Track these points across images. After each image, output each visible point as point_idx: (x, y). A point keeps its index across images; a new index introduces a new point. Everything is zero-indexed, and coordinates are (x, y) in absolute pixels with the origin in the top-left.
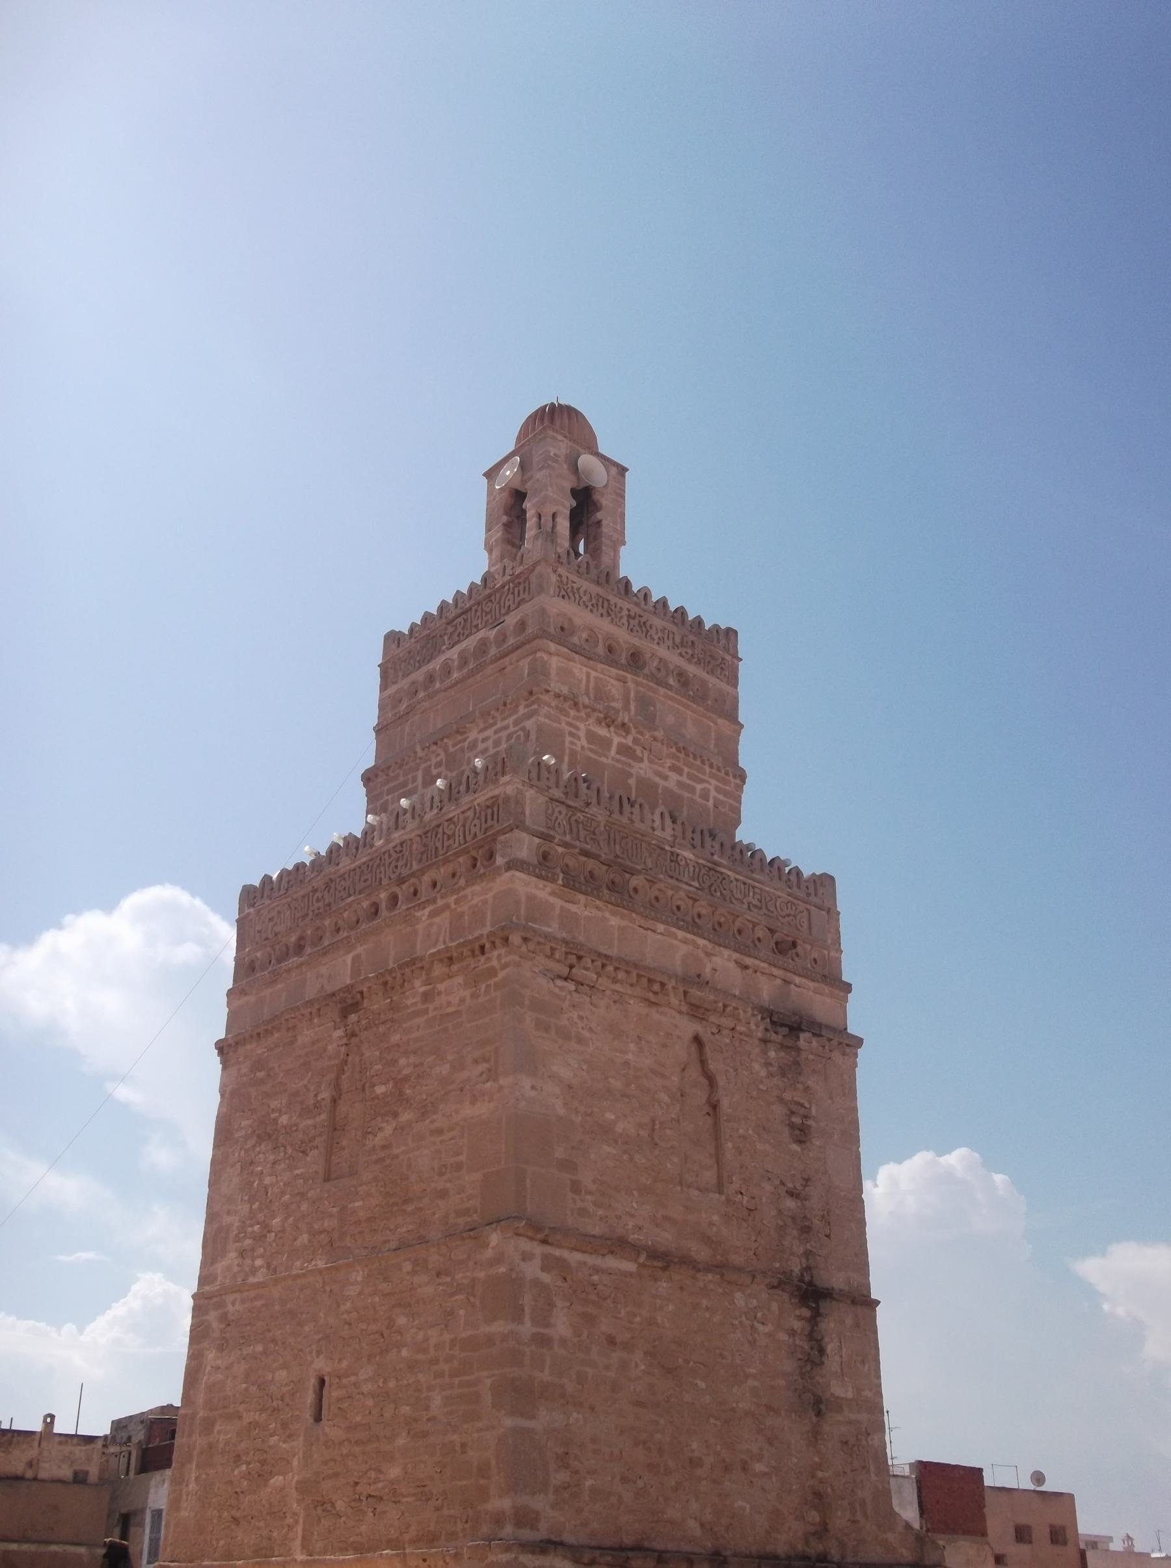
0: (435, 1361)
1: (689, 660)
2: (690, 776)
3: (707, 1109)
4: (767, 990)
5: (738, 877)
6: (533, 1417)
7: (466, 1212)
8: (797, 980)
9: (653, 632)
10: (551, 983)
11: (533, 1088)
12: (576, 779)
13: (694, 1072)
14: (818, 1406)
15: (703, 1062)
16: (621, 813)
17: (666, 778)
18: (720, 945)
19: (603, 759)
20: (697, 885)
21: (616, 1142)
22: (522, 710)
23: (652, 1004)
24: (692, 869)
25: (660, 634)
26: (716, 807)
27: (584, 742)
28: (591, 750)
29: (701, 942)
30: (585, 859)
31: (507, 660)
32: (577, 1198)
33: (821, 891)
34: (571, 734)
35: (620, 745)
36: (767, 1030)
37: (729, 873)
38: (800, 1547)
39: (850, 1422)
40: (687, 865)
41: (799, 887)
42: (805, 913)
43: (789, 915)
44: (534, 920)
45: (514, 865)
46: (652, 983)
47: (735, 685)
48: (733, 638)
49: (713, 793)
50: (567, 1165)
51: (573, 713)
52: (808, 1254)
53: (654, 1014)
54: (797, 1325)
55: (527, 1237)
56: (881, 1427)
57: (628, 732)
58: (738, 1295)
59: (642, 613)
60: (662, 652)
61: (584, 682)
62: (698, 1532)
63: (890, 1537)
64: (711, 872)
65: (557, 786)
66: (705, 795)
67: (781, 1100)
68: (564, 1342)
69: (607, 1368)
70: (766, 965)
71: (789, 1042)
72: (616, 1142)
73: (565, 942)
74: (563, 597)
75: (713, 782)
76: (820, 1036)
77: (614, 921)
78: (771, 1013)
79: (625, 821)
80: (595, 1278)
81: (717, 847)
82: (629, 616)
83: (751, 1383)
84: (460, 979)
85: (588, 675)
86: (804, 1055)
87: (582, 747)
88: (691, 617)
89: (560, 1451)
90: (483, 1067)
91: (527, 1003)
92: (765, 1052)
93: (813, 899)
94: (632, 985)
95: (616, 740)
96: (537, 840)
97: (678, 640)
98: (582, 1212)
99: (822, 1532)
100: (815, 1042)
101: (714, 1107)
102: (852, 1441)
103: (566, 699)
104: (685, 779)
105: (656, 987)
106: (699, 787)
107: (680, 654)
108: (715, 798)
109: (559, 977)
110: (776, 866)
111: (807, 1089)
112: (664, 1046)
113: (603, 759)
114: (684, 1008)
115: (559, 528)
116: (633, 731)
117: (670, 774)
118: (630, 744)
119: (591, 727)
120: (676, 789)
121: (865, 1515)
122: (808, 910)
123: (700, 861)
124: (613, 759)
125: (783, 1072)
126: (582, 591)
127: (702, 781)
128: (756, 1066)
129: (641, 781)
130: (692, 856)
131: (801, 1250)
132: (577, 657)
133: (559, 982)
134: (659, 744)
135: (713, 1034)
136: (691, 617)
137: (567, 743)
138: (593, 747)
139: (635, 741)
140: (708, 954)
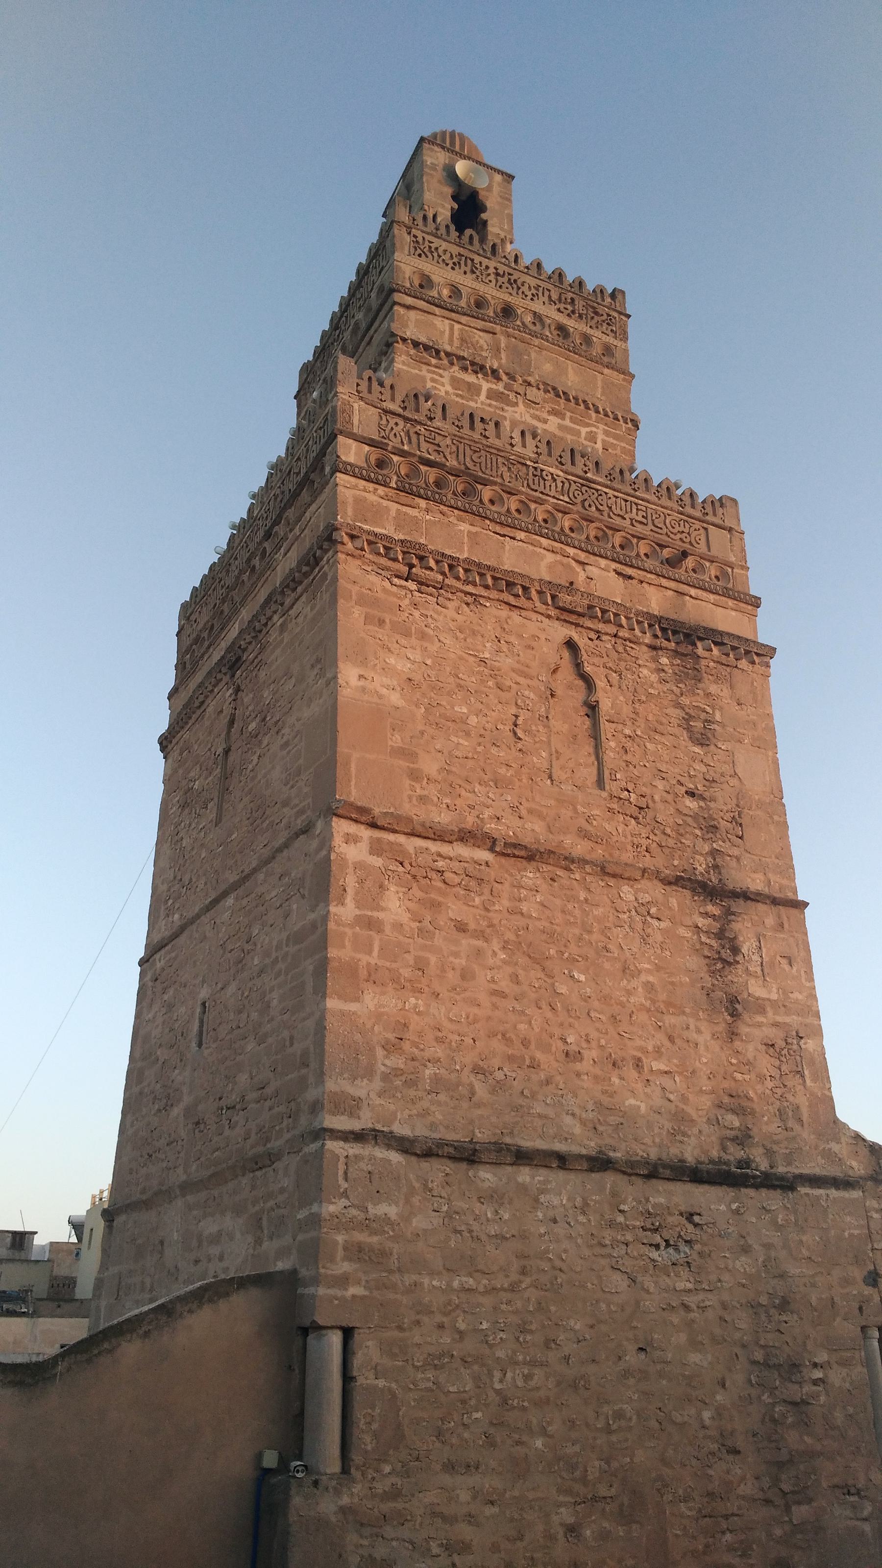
1: (568, 315)
2: (572, 420)
3: (584, 710)
4: (656, 600)
5: (616, 494)
6: (357, 999)
8: (693, 592)
9: (525, 288)
10: (387, 584)
11: (361, 677)
12: (416, 396)
13: (567, 673)
14: (734, 1007)
17: (545, 421)
18: (595, 554)
20: (567, 500)
24: (560, 485)
25: (534, 291)
27: (449, 388)
28: (457, 395)
29: (571, 551)
30: (427, 468)
32: (418, 786)
33: (720, 511)
34: (433, 380)
35: (489, 390)
37: (607, 490)
38: (715, 1154)
39: (776, 1025)
40: (555, 480)
41: (693, 506)
42: (702, 531)
43: (683, 532)
47: (625, 338)
48: (620, 297)
49: (600, 437)
51: (434, 361)
52: (714, 853)
54: (701, 922)
55: (351, 819)
56: (817, 1032)
58: (625, 888)
59: (511, 271)
60: (538, 306)
61: (447, 332)
62: (577, 1130)
63: (835, 1147)
64: (584, 489)
65: (393, 399)
66: (592, 437)
67: (678, 705)
68: (398, 926)
69: (456, 955)
70: (653, 576)
71: (682, 649)
74: (420, 255)
75: (601, 426)
77: (464, 527)
78: (660, 619)
79: (476, 436)
80: (441, 864)
81: (591, 466)
82: (497, 274)
83: (643, 978)
85: (452, 328)
86: (703, 662)
87: (447, 393)
88: (570, 278)
89: (391, 1036)
91: (354, 597)
92: (656, 660)
93: (709, 518)
94: (487, 587)
95: (485, 386)
96: (367, 448)
97: (555, 297)
99: (743, 1138)
100: (716, 651)
101: (592, 709)
102: (780, 1043)
103: (427, 348)
104: (567, 422)
106: (584, 431)
107: (559, 310)
108: (603, 441)
110: (664, 486)
111: (708, 695)
114: (553, 612)
116: (504, 377)
117: (551, 418)
118: (502, 390)
119: (456, 374)
121: (800, 1121)
122: (706, 529)
123: (570, 477)
124: (482, 403)
126: (440, 250)
127: (588, 425)
128: (645, 672)
130: (561, 474)
131: (706, 848)
132: (437, 310)
133: (396, 581)
134: (534, 389)
135: (590, 639)
136: (570, 278)
138: (460, 392)
139: (507, 387)
140: (582, 563)
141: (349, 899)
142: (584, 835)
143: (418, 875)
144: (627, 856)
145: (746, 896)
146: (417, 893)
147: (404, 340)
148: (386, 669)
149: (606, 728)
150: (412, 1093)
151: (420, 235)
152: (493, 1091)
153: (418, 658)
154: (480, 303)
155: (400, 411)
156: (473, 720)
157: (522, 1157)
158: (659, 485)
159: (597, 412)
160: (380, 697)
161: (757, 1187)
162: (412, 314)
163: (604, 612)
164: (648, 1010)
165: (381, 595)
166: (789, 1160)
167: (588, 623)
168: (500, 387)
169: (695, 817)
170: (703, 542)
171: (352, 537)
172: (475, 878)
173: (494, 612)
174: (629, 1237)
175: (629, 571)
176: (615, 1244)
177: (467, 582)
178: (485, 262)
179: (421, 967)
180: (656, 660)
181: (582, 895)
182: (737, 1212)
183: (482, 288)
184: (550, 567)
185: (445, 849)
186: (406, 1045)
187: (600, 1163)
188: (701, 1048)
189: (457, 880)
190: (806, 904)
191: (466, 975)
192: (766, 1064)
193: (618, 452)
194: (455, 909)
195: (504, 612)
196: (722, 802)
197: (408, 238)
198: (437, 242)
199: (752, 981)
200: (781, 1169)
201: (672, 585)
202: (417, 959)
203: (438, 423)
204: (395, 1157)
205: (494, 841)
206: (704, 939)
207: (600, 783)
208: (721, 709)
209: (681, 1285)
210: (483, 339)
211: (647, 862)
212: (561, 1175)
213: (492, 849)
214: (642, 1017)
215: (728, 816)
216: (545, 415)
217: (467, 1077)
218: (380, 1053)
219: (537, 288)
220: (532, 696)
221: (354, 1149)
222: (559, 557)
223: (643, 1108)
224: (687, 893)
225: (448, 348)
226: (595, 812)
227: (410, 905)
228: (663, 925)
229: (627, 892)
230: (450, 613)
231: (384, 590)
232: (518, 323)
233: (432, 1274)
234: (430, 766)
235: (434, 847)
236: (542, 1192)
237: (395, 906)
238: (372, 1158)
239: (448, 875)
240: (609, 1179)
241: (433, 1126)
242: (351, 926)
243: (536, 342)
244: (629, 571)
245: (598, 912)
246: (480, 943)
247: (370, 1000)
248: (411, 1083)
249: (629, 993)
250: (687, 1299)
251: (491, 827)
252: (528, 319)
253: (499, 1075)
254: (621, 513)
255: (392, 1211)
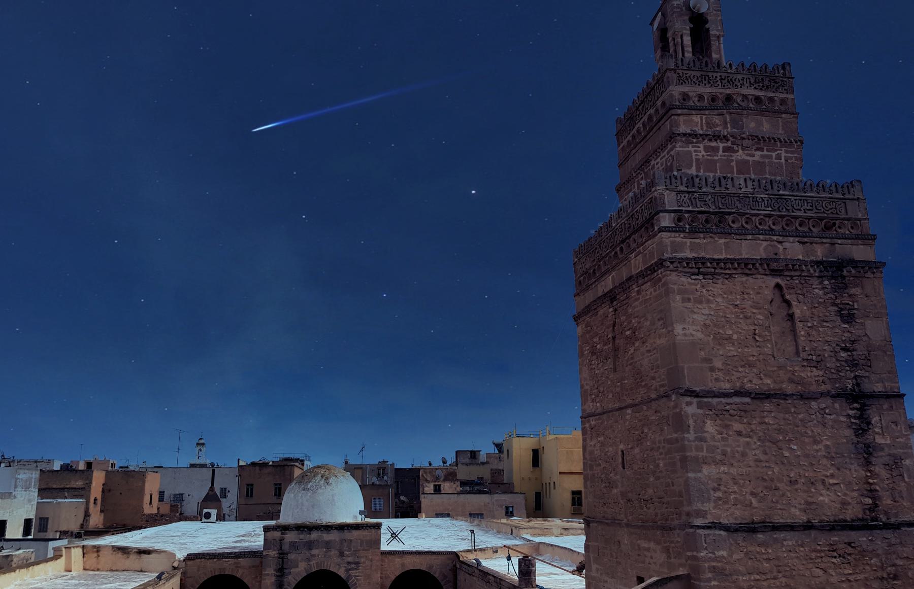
0: (659, 447)
2: (768, 151)
4: (820, 252)
6: (700, 471)
7: (662, 386)
8: (839, 241)
10: (689, 280)
13: (778, 300)
15: (783, 296)
16: (720, 186)
17: (753, 156)
19: (716, 158)
21: (733, 344)
22: (669, 147)
23: (747, 275)
26: (786, 161)
29: (775, 238)
31: (660, 124)
34: (695, 151)
35: (724, 147)
36: (821, 271)
39: (889, 455)
41: (837, 192)
44: (676, 252)
45: (663, 229)
46: (746, 266)
48: (788, 68)
49: (783, 155)
50: (708, 360)
52: (856, 377)
53: (750, 279)
54: (851, 412)
57: (728, 140)
58: (813, 403)
60: (745, 91)
62: (798, 513)
67: (834, 304)
69: (739, 446)
72: (733, 344)
73: (695, 258)
76: (857, 267)
77: (722, 241)
79: (723, 190)
80: (728, 407)
82: (721, 79)
84: (649, 284)
85: (701, 120)
88: (759, 65)
90: (661, 322)
92: (821, 283)
93: (847, 196)
94: (735, 269)
95: (721, 145)
97: (752, 81)
98: (717, 380)
99: (874, 507)
101: (791, 317)
103: (690, 135)
104: (765, 153)
105: (750, 266)
106: (774, 154)
109: (694, 274)
111: (850, 296)
112: (759, 293)
113: (716, 158)
115: (685, 42)
116: (731, 138)
120: (761, 160)
125: (834, 290)
127: (776, 150)
129: (738, 162)
131: (852, 375)
132: (693, 112)
133: (693, 277)
137: (694, 157)
139: (733, 143)
141: (691, 431)
142: (791, 381)
143: (719, 414)
144: (813, 388)
145: (873, 396)
146: (718, 422)
147: (679, 134)
148: (694, 322)
149: (799, 325)
150: (726, 507)
151: (680, 72)
152: (760, 502)
153: (707, 312)
154: (714, 99)
155: (686, 189)
156: (735, 337)
157: (776, 528)
158: (818, 185)
159: (781, 141)
160: (692, 335)
161: (881, 529)
162: (681, 118)
163: (793, 266)
164: (827, 457)
165: (687, 287)
166: (896, 515)
167: (786, 273)
168: (729, 144)
169: (846, 361)
170: (843, 211)
171: (672, 263)
172: (744, 411)
173: (740, 279)
174: (823, 554)
175: (806, 240)
176: (817, 557)
177: (725, 269)
178: (715, 75)
179: (724, 454)
180: (821, 283)
181: (793, 410)
182: (871, 540)
183: (714, 90)
184: (765, 249)
185: (729, 400)
186: (722, 488)
187: (808, 527)
188: (853, 471)
189: (735, 413)
190: (904, 395)
191: (744, 455)
192: (884, 474)
193: (793, 160)
194: (737, 426)
195: (744, 279)
196: (860, 350)
197: (675, 76)
198: (689, 73)
199: (877, 436)
200: (893, 520)
201: (828, 240)
202: (723, 450)
203: (704, 190)
204: (723, 533)
205: (750, 393)
206: (853, 420)
207: (797, 353)
208: (857, 301)
209: (846, 572)
210: (717, 120)
211: (823, 387)
212: (792, 533)
213: (749, 397)
214: (824, 461)
215: (863, 357)
216: (753, 152)
217: (749, 497)
218: (712, 492)
219: (743, 79)
220: (762, 317)
221: (707, 532)
222: (769, 243)
223: (827, 500)
224: (844, 400)
225: (701, 132)
226: (797, 368)
227: (717, 428)
228: (832, 417)
229: (814, 404)
230: (718, 287)
231: (689, 283)
232: (736, 105)
233: (743, 575)
234: (718, 364)
235: (723, 400)
236: (785, 540)
237: (710, 427)
238: (714, 535)
239: (732, 412)
240: (813, 533)
241: (736, 519)
242: (694, 441)
243: (745, 112)
244: (806, 240)
245: (801, 416)
246: (748, 439)
247: (706, 470)
248: (726, 503)
249: (817, 451)
250: (849, 577)
251: (748, 386)
252: (739, 99)
253: (762, 495)
254: (798, 207)
255: (724, 553)
